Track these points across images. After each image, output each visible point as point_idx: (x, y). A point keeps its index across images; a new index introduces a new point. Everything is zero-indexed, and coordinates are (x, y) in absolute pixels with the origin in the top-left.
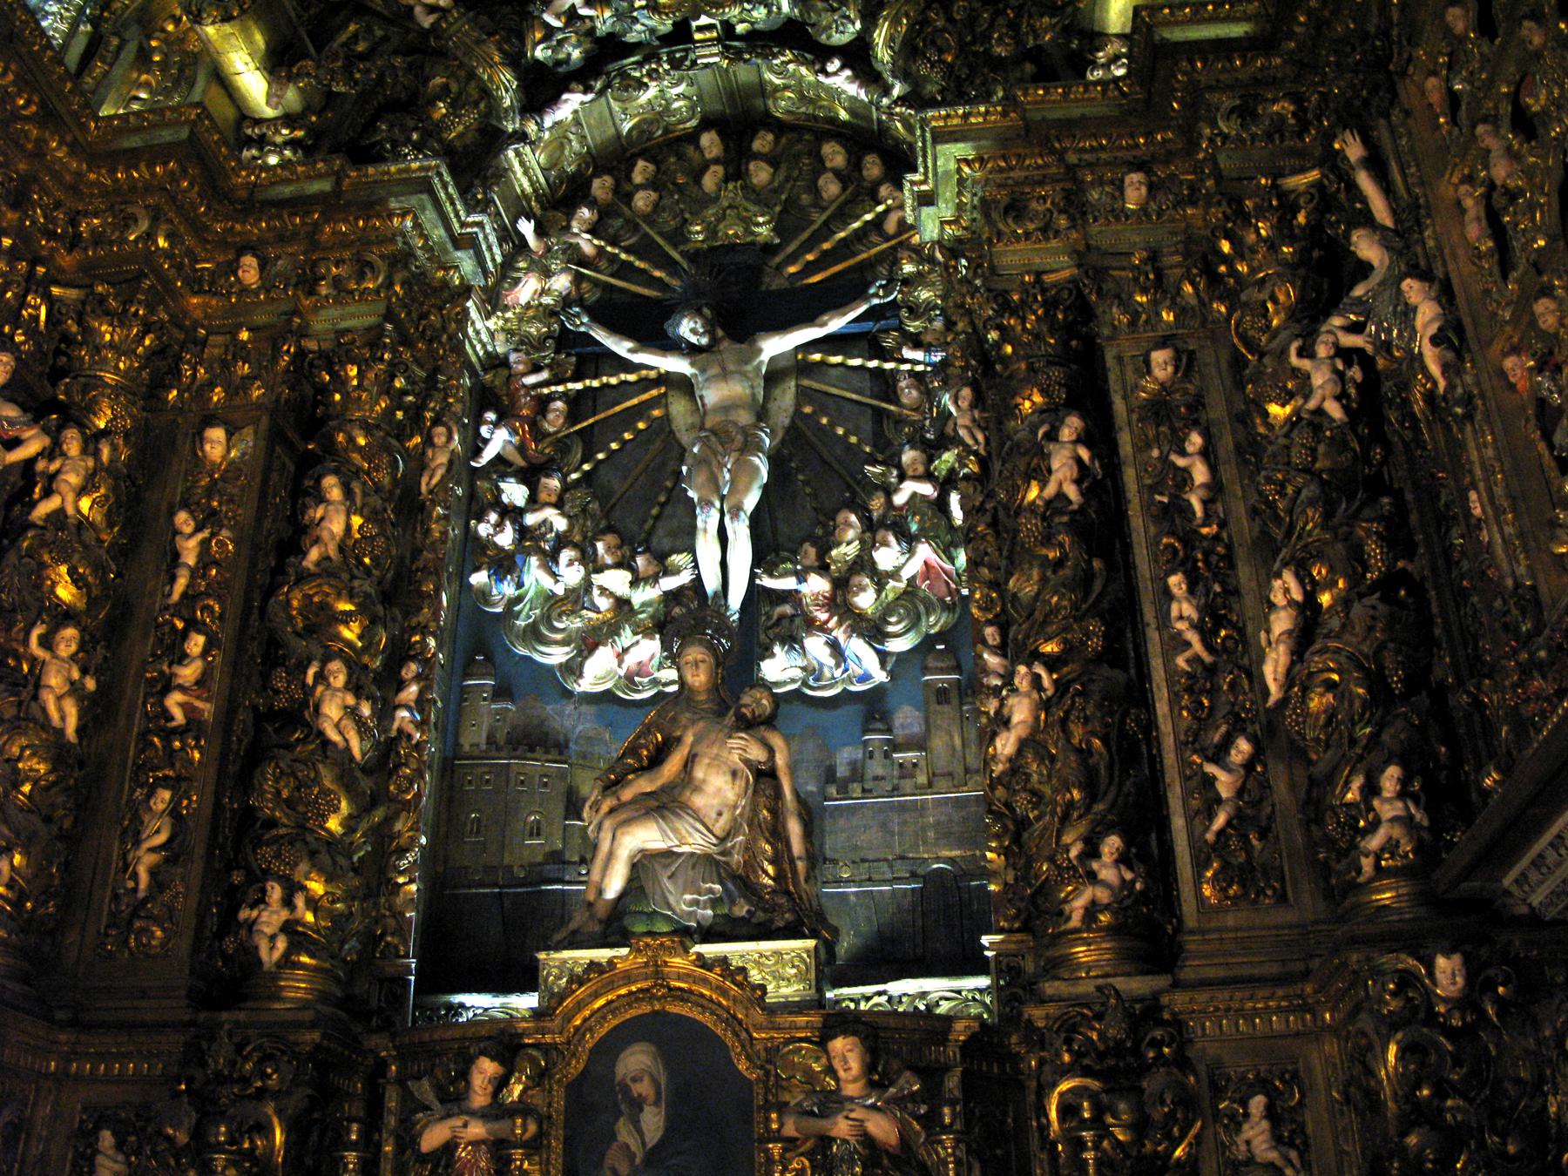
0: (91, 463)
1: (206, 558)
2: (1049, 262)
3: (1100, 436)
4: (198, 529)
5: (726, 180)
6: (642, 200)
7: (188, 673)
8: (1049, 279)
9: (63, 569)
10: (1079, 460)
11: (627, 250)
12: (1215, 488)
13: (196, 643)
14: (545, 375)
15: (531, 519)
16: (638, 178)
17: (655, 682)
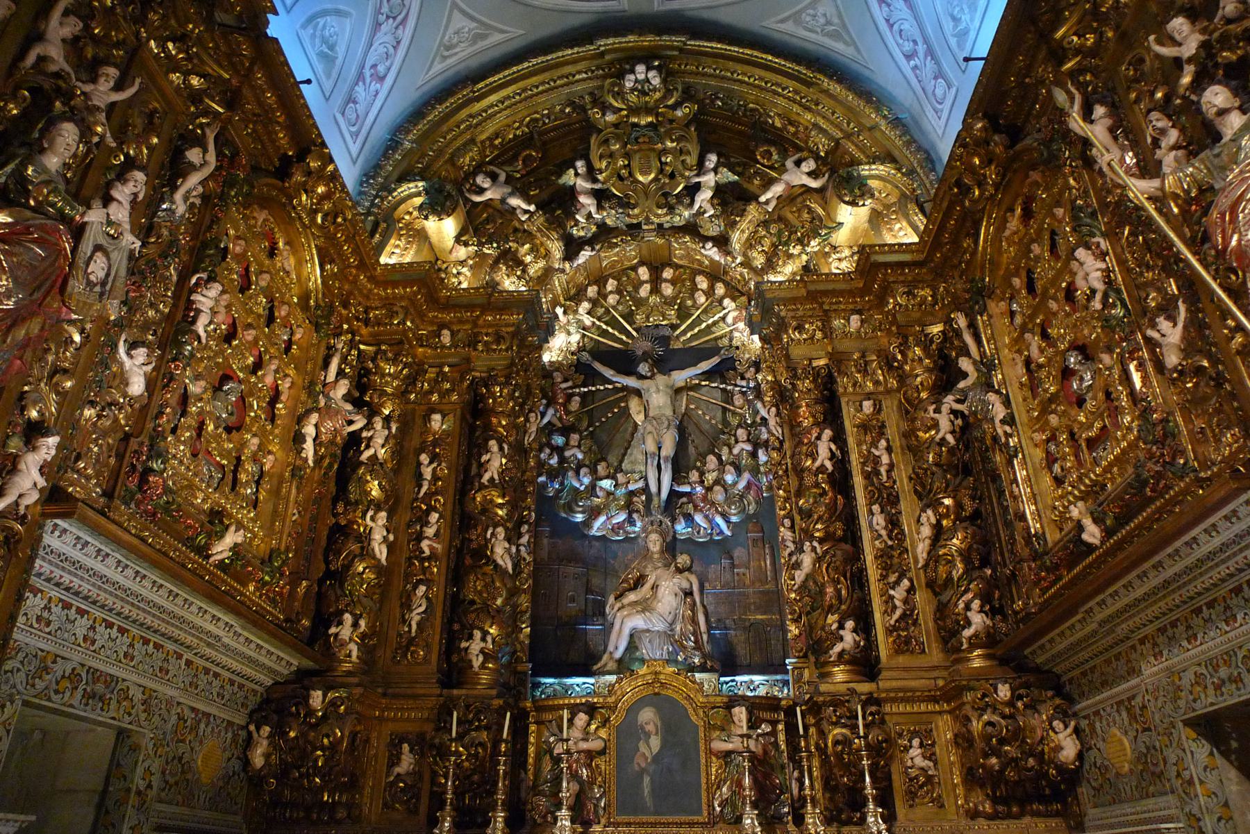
0: (386, 432)
1: (435, 478)
2: (814, 354)
3: (839, 438)
4: (431, 463)
5: (651, 292)
6: (612, 299)
7: (430, 531)
8: (815, 364)
9: (376, 483)
10: (831, 450)
11: (606, 323)
12: (891, 466)
13: (434, 517)
14: (570, 384)
15: (567, 454)
16: (609, 288)
17: (626, 532)
